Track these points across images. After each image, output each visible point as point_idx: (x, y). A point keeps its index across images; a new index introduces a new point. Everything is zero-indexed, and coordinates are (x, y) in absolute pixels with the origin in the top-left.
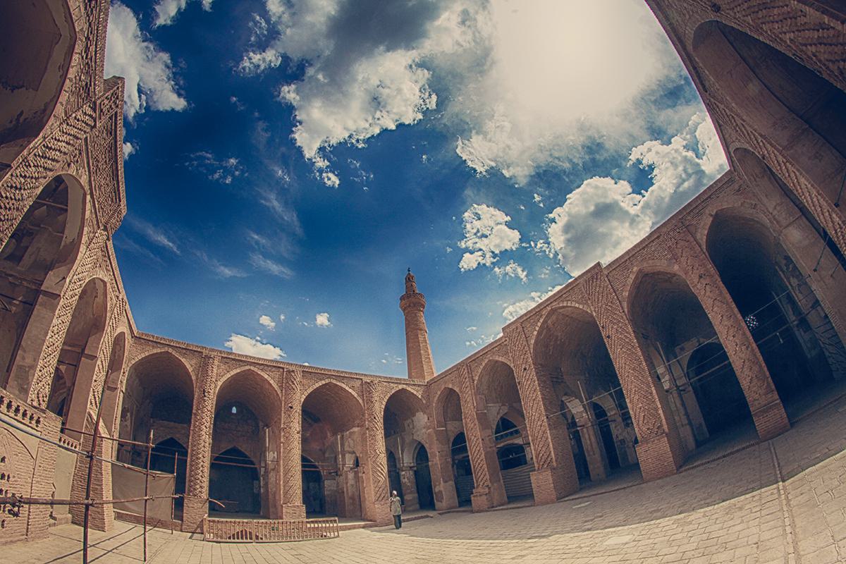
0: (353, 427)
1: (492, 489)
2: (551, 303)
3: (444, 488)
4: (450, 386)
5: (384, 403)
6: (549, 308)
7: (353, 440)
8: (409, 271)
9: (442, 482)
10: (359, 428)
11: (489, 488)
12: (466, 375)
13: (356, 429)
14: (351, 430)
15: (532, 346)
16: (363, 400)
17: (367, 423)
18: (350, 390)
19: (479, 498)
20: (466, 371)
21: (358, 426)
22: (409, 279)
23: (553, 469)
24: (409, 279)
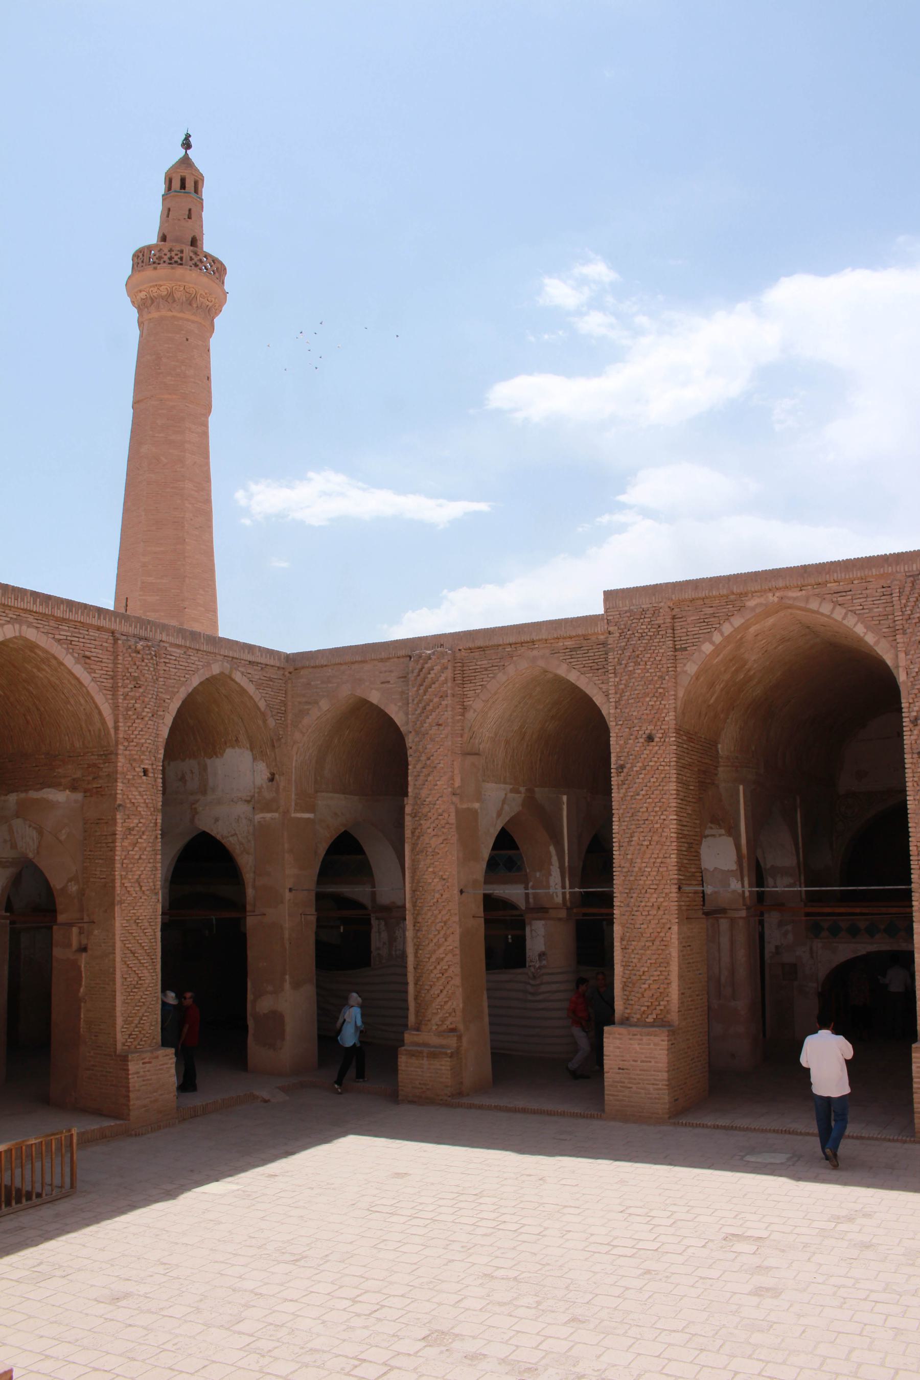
0: (56, 785)
1: (464, 1039)
2: (787, 588)
3: (283, 998)
4: (375, 697)
5: (169, 720)
6: (772, 598)
7: (40, 832)
8: (187, 145)
9: (287, 986)
10: (79, 796)
11: (460, 1038)
12: (448, 688)
13: (59, 796)
14: (33, 794)
15: (685, 681)
16: (115, 707)
17: (120, 786)
18: (79, 671)
19: (425, 1062)
20: (449, 673)
21: (74, 788)
22: (184, 184)
23: (673, 1032)
24: (183, 186)
